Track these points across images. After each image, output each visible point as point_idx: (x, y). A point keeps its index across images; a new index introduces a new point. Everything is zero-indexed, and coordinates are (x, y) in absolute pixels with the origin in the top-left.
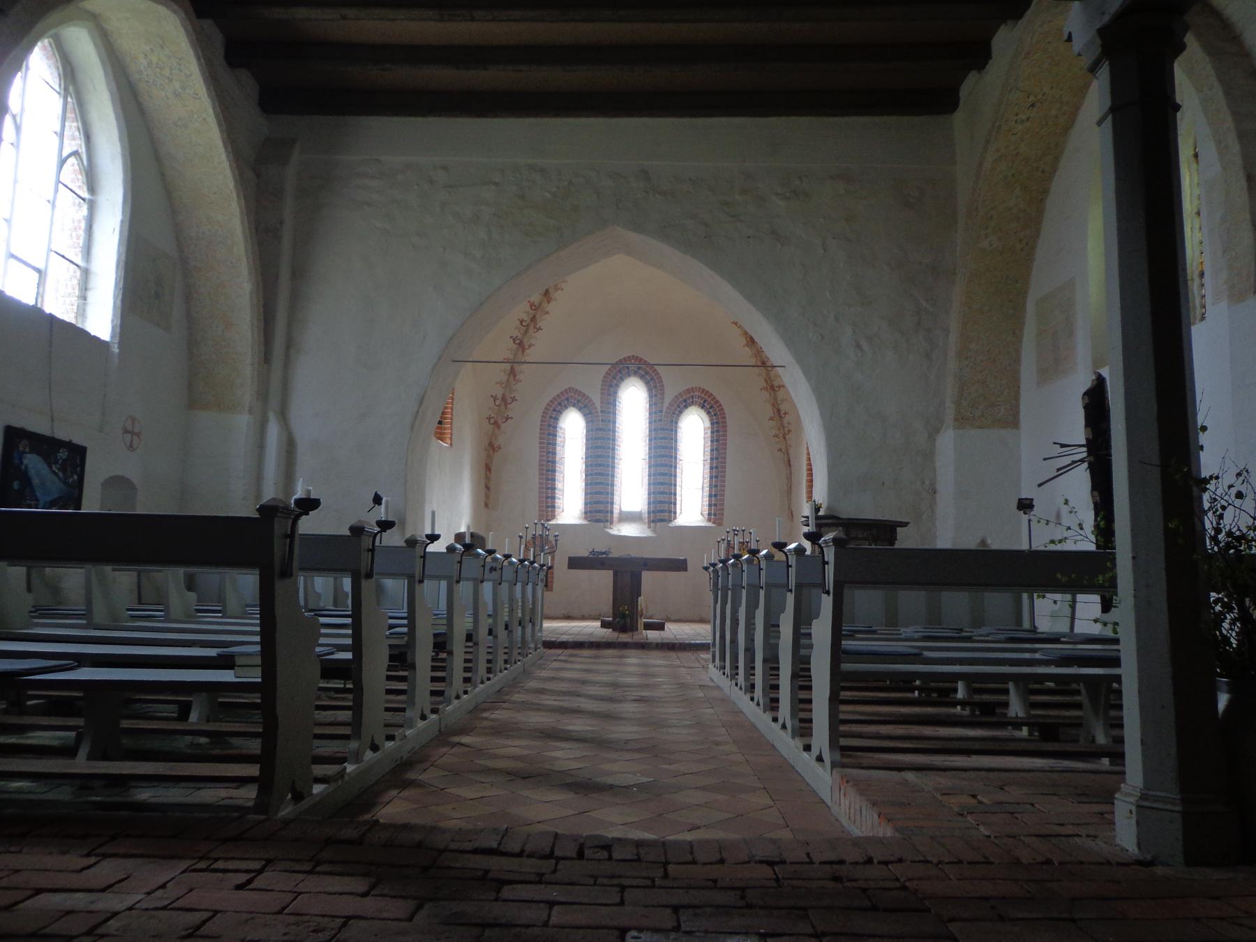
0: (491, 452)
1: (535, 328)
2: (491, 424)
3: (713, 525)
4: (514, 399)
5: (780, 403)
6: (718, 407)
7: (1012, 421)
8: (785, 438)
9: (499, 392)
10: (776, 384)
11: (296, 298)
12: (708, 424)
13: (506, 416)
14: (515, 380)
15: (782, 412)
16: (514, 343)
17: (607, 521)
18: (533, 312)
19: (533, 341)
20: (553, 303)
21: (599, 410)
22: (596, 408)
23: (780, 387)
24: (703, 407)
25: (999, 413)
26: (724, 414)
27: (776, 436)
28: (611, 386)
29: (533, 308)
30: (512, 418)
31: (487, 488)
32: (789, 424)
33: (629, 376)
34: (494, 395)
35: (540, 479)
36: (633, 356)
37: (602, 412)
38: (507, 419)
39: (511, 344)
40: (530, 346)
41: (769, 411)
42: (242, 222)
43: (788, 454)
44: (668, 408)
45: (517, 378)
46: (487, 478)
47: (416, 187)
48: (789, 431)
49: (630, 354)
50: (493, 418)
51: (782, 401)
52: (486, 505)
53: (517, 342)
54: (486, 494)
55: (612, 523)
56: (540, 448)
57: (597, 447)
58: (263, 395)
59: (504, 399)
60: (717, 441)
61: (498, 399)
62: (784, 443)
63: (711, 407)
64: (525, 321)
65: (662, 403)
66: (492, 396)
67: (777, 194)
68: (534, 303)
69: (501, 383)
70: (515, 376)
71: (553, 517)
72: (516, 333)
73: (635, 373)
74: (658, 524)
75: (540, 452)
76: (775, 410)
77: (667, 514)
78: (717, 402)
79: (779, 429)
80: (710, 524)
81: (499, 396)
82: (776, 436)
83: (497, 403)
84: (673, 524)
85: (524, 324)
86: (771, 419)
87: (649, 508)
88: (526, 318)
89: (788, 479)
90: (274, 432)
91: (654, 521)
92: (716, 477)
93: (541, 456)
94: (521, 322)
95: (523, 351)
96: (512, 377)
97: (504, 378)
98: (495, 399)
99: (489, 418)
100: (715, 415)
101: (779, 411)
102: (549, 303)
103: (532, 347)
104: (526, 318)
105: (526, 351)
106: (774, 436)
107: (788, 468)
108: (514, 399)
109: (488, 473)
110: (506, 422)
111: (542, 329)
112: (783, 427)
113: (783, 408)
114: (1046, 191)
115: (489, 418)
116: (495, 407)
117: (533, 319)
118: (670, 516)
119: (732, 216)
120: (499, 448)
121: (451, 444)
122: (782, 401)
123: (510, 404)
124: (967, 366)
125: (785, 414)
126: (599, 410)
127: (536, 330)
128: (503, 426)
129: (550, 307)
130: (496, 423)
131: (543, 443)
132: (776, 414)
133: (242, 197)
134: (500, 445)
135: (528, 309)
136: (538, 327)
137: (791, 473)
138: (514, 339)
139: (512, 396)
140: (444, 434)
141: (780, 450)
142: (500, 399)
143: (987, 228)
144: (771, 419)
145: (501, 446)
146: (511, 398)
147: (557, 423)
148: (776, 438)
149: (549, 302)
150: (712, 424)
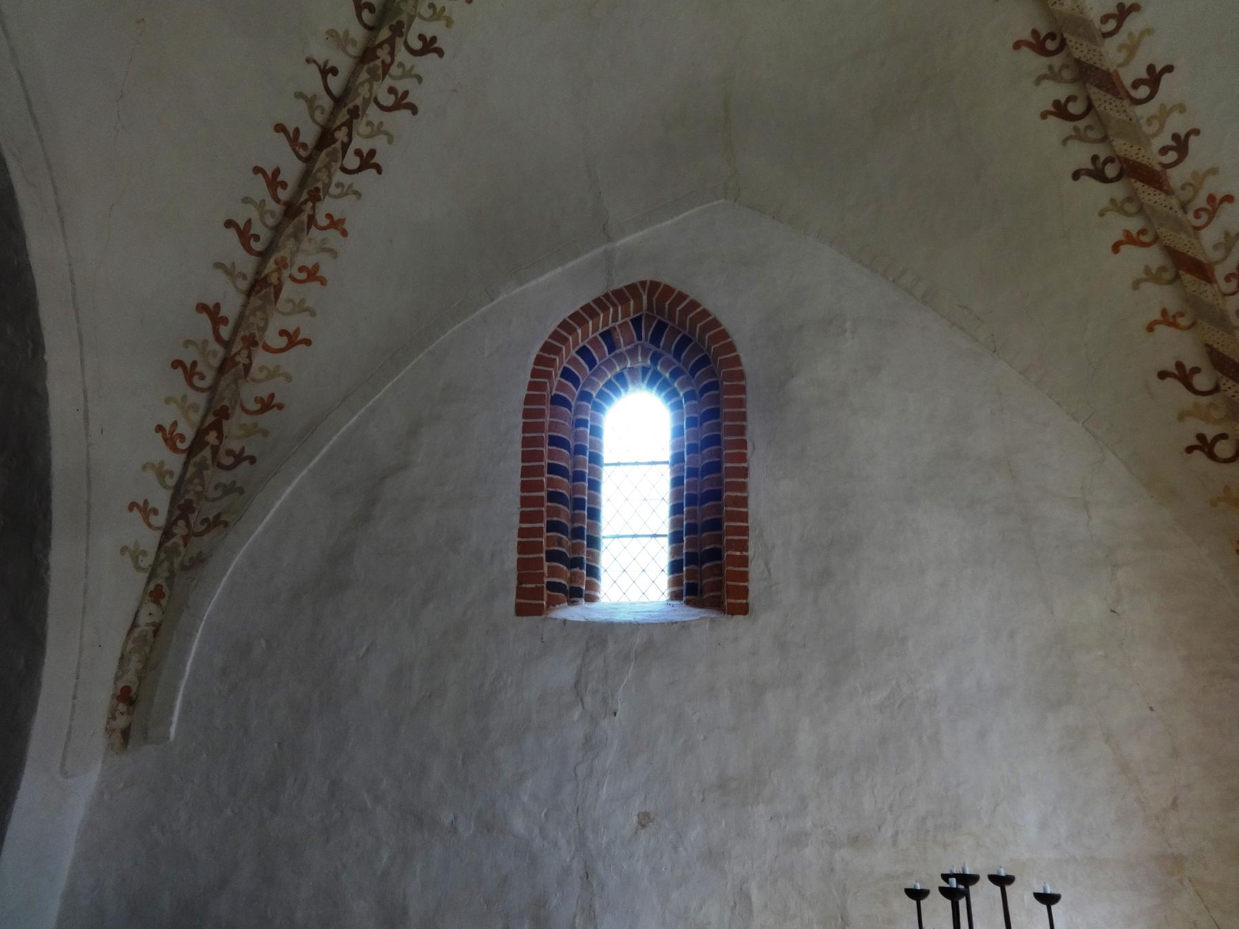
16: (1105, 180)
18: (1056, 61)
29: (1051, 45)
34: (1170, 367)
39: (1097, 193)
40: (1181, 145)
50: (1223, 436)
61: (1196, 370)
66: (1163, 375)
68: (1035, 33)
69: (1168, 319)
83: (1202, 382)
85: (1075, 108)
94: (1060, 110)
96: (1187, 278)
98: (1184, 375)
103: (1194, 142)
104: (1060, 92)
105: (1176, 177)
115: (1205, 445)
135: (1038, 63)
138: (1090, 173)
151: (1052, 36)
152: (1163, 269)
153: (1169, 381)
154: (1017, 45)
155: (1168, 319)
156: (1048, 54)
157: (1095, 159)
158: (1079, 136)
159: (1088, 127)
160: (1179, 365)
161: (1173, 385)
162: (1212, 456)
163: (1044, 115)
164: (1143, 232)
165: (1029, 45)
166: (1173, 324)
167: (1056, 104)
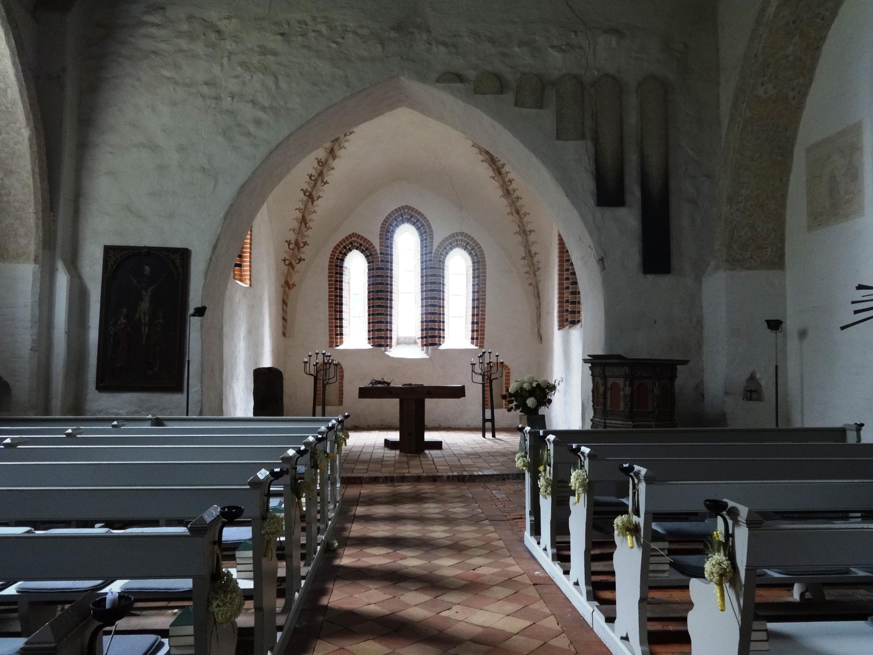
0: (287, 289)
1: (322, 181)
2: (286, 265)
3: (478, 348)
4: (305, 244)
5: (531, 245)
6: (478, 248)
7: (778, 262)
8: (535, 275)
9: (292, 237)
10: (528, 229)
11: (83, 147)
12: (470, 263)
13: (299, 258)
14: (306, 227)
15: (533, 252)
16: (305, 195)
17: (387, 346)
19: (321, 194)
20: (337, 160)
21: (379, 252)
22: (376, 250)
23: (531, 231)
24: (465, 249)
25: (766, 254)
26: (484, 254)
27: (527, 273)
28: (388, 231)
29: (320, 164)
30: (304, 260)
31: (284, 319)
32: (539, 262)
33: (403, 223)
35: (329, 311)
36: (406, 206)
37: (381, 253)
38: (300, 260)
39: (301, 195)
40: (319, 197)
41: (522, 252)
42: (14, 64)
43: (537, 288)
44: (436, 250)
45: (308, 225)
46: (284, 311)
47: (203, 37)
48: (539, 269)
49: (404, 204)
50: (288, 260)
51: (533, 243)
52: (284, 334)
53: (307, 194)
54: (283, 325)
55: (391, 347)
56: (329, 284)
57: (377, 284)
58: (48, 243)
59: (297, 243)
60: (478, 277)
61: (292, 243)
62: (534, 279)
63: (472, 249)
64: (314, 176)
65: (432, 246)
66: (286, 241)
67: (553, 47)
68: (321, 159)
69: (294, 230)
70: (306, 224)
71: (341, 342)
72: (306, 187)
73: (408, 221)
74: (430, 347)
75: (329, 288)
76: (527, 251)
77: (437, 339)
78: (478, 244)
79: (530, 267)
80: (473, 347)
81: (293, 241)
82: (527, 273)
83: (292, 246)
84: (441, 347)
85: (313, 178)
86: (524, 258)
87: (422, 334)
88: (314, 173)
89: (537, 308)
90: (62, 280)
91: (426, 345)
92: (478, 307)
93: (330, 292)
94: (311, 176)
95: (313, 202)
96: (303, 224)
97: (296, 225)
98: (289, 243)
99: (284, 260)
100: (476, 255)
101: (530, 251)
102: (334, 160)
104: (314, 173)
105: (316, 202)
106: (525, 273)
107: (538, 299)
108: (305, 244)
109: (285, 306)
110: (299, 263)
111: (328, 183)
112: (533, 264)
113: (534, 249)
114: (823, 39)
115: (284, 260)
116: (289, 250)
117: (321, 174)
118: (440, 341)
119: (511, 67)
120: (294, 285)
121: (250, 285)
122: (533, 243)
123: (302, 247)
124: (738, 210)
125: (535, 254)
126: (379, 252)
127: (323, 184)
128: (297, 267)
129: (336, 163)
130: (290, 264)
131: (332, 281)
132: (527, 254)
133: (11, 36)
134: (294, 283)
135: (316, 164)
136: (325, 181)
137: (540, 304)
139: (304, 241)
140: (244, 275)
141: (531, 284)
142: (294, 243)
143: (764, 76)
144: (524, 258)
145: (295, 284)
146: (303, 242)
147: (343, 264)
148: (526, 274)
149: (334, 159)
150: (474, 263)
151: (322, 163)
152: (299, 219)
153: (286, 243)
154: (316, 158)
155: (294, 230)
156: (319, 165)
157: (307, 189)
158: (309, 183)
159: (312, 183)
160: (290, 241)
161: (287, 244)
162: (285, 263)
163: (308, 175)
164: (302, 209)
165: (318, 160)
166: (294, 232)
167: (311, 174)
